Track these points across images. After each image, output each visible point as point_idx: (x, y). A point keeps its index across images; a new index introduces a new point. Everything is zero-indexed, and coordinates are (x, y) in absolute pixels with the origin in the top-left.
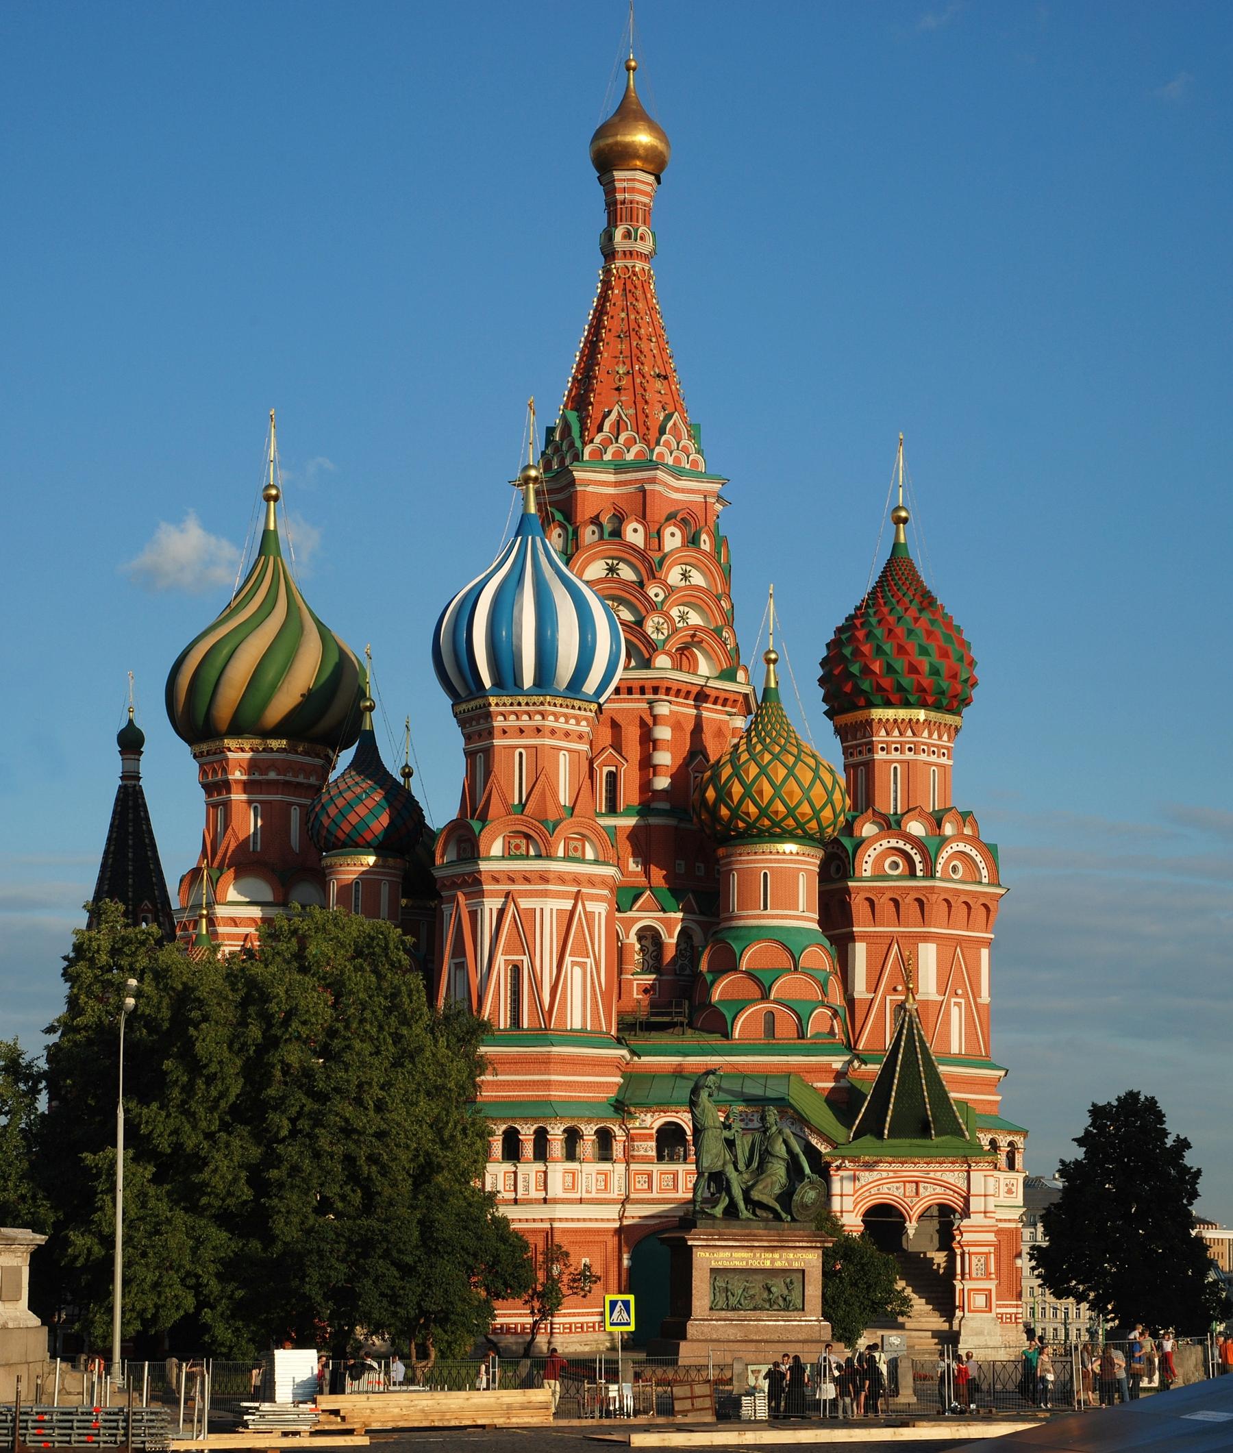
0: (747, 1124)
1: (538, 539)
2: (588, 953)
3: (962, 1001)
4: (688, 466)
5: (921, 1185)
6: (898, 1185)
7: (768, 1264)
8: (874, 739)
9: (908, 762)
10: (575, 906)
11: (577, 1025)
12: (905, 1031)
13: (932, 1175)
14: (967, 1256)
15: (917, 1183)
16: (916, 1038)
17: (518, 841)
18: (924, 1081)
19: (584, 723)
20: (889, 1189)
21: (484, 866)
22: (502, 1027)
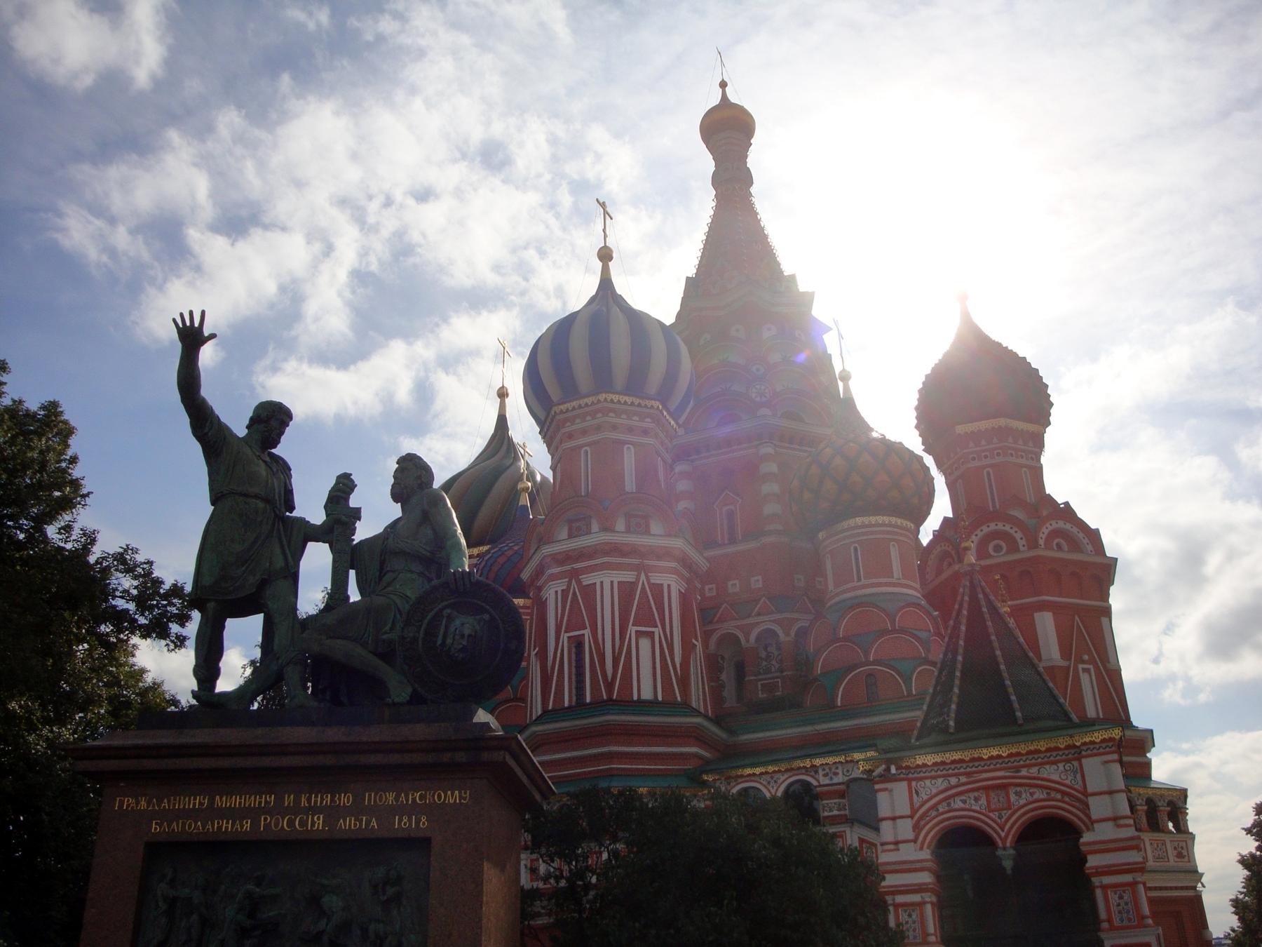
0: (831, 779)
2: (655, 621)
3: (1091, 667)
5: (1012, 790)
6: (976, 794)
7: (319, 822)
8: (965, 451)
11: (647, 694)
12: (966, 598)
13: (1024, 772)
14: (1099, 893)
15: (1004, 787)
16: (983, 603)
19: (649, 420)
21: (547, 550)
22: (566, 704)
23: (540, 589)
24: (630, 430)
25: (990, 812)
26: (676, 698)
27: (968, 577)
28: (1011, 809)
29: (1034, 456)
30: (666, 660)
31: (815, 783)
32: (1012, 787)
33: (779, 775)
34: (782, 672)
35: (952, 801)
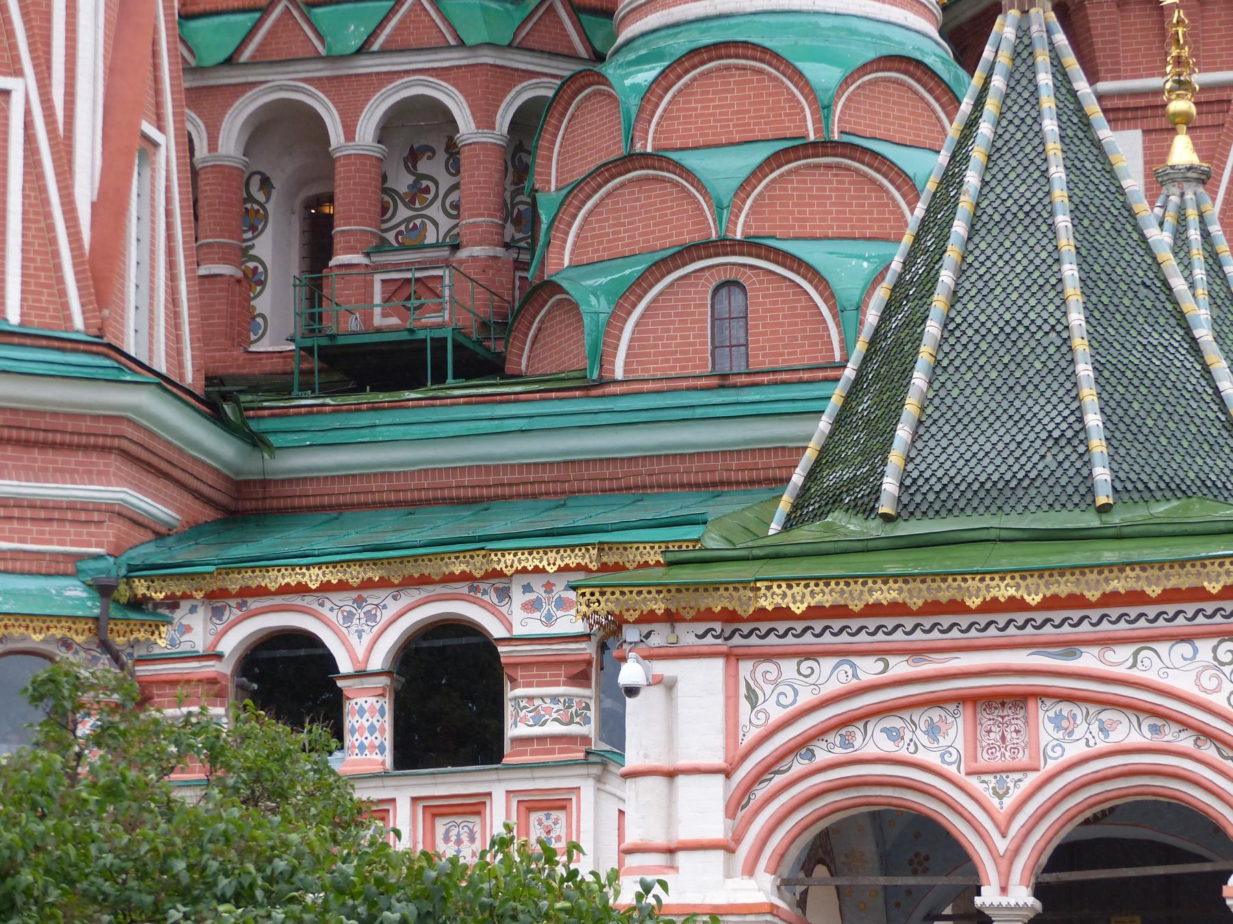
0: (549, 619)
2: (16, 59)
6: (935, 714)
12: (998, 82)
13: (1088, 660)
16: (1048, 102)
18: (1070, 271)
25: (968, 774)
26: (68, 318)
27: (1014, 13)
28: (1037, 770)
30: (43, 190)
31: (496, 630)
32: (1048, 702)
33: (382, 593)
34: (456, 247)
35: (857, 731)
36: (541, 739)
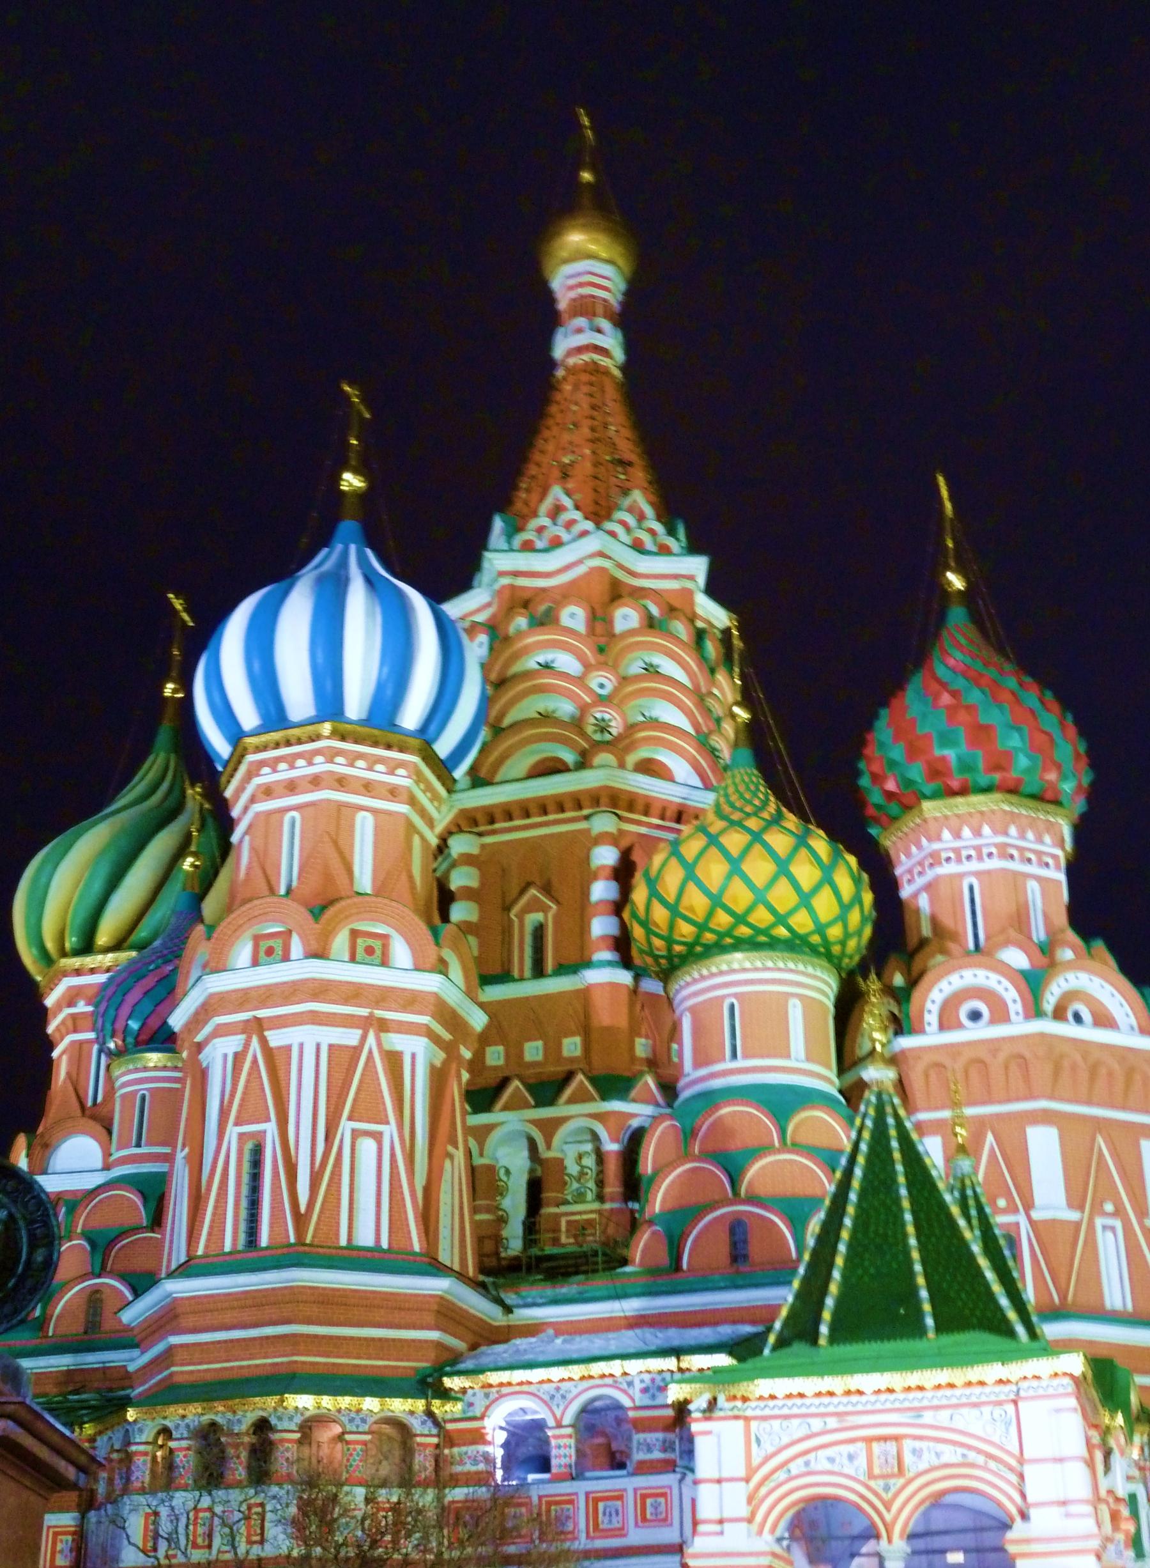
0: (653, 1397)
1: (353, 548)
2: (387, 1116)
3: (1118, 1224)
4: (654, 549)
5: (908, 1444)
6: (851, 1448)
8: (936, 846)
9: (988, 872)
10: (364, 1038)
11: (365, 1237)
12: (869, 1123)
13: (928, 1417)
15: (897, 1438)
16: (893, 1132)
17: (271, 943)
18: (908, 1217)
20: (831, 1460)
22: (228, 1248)
23: (200, 1047)
24: (368, 788)
29: (1050, 861)
31: (627, 1402)
35: (811, 1456)
36: (651, 1462)
